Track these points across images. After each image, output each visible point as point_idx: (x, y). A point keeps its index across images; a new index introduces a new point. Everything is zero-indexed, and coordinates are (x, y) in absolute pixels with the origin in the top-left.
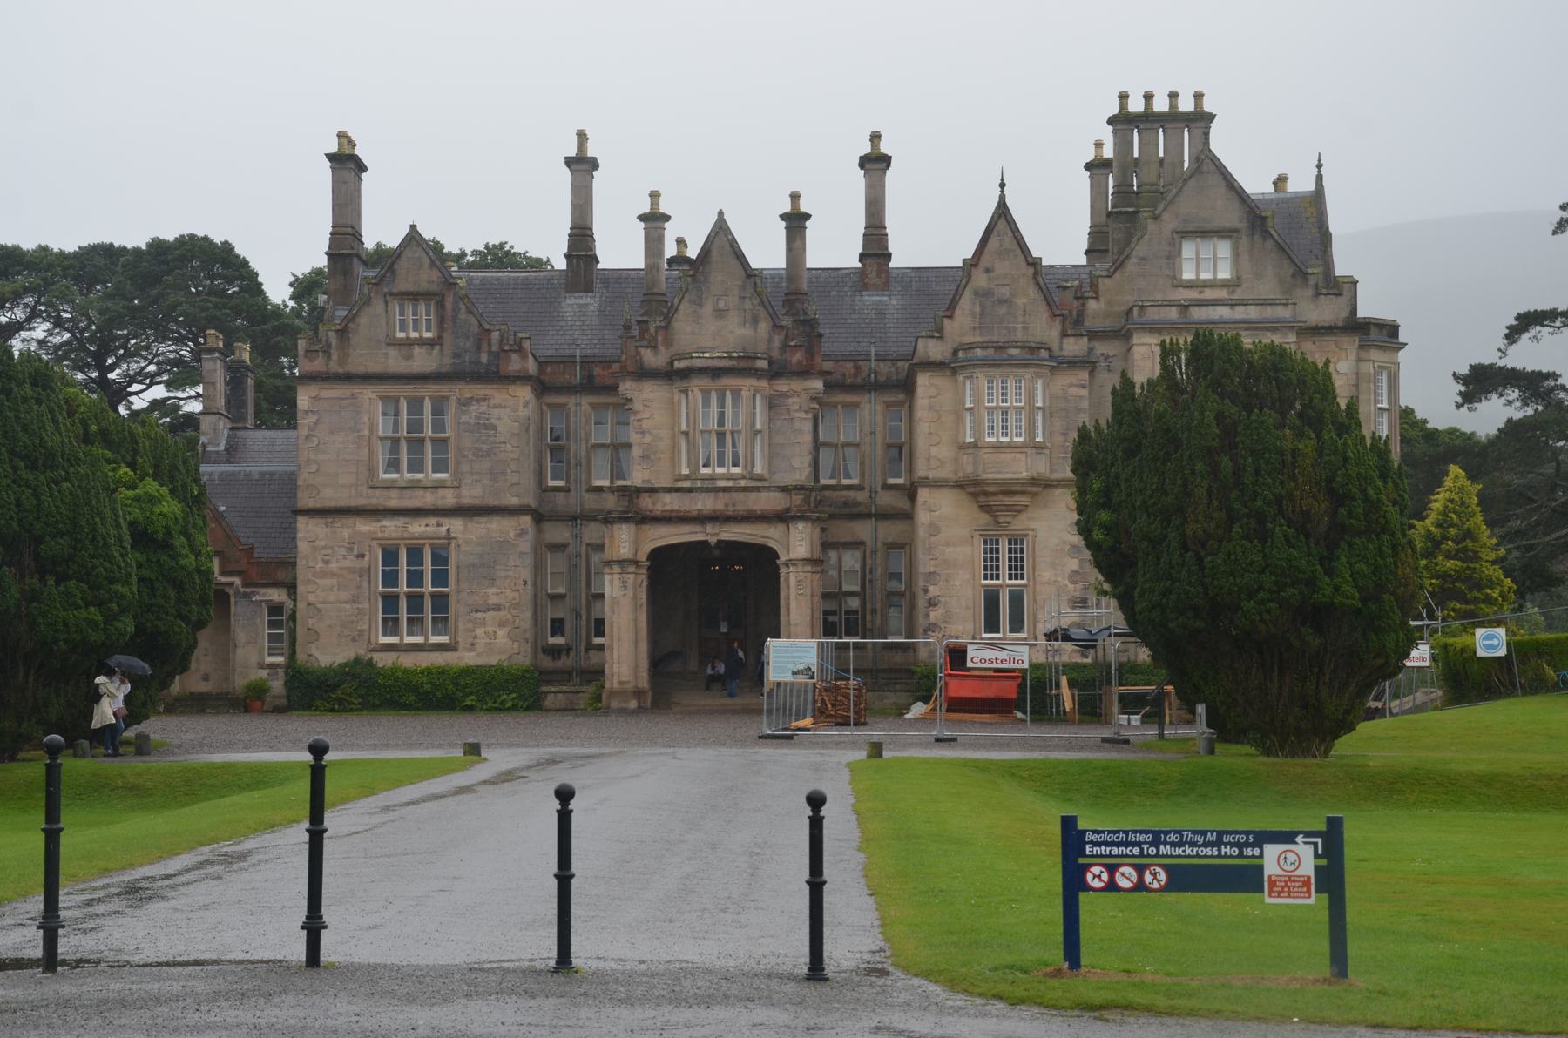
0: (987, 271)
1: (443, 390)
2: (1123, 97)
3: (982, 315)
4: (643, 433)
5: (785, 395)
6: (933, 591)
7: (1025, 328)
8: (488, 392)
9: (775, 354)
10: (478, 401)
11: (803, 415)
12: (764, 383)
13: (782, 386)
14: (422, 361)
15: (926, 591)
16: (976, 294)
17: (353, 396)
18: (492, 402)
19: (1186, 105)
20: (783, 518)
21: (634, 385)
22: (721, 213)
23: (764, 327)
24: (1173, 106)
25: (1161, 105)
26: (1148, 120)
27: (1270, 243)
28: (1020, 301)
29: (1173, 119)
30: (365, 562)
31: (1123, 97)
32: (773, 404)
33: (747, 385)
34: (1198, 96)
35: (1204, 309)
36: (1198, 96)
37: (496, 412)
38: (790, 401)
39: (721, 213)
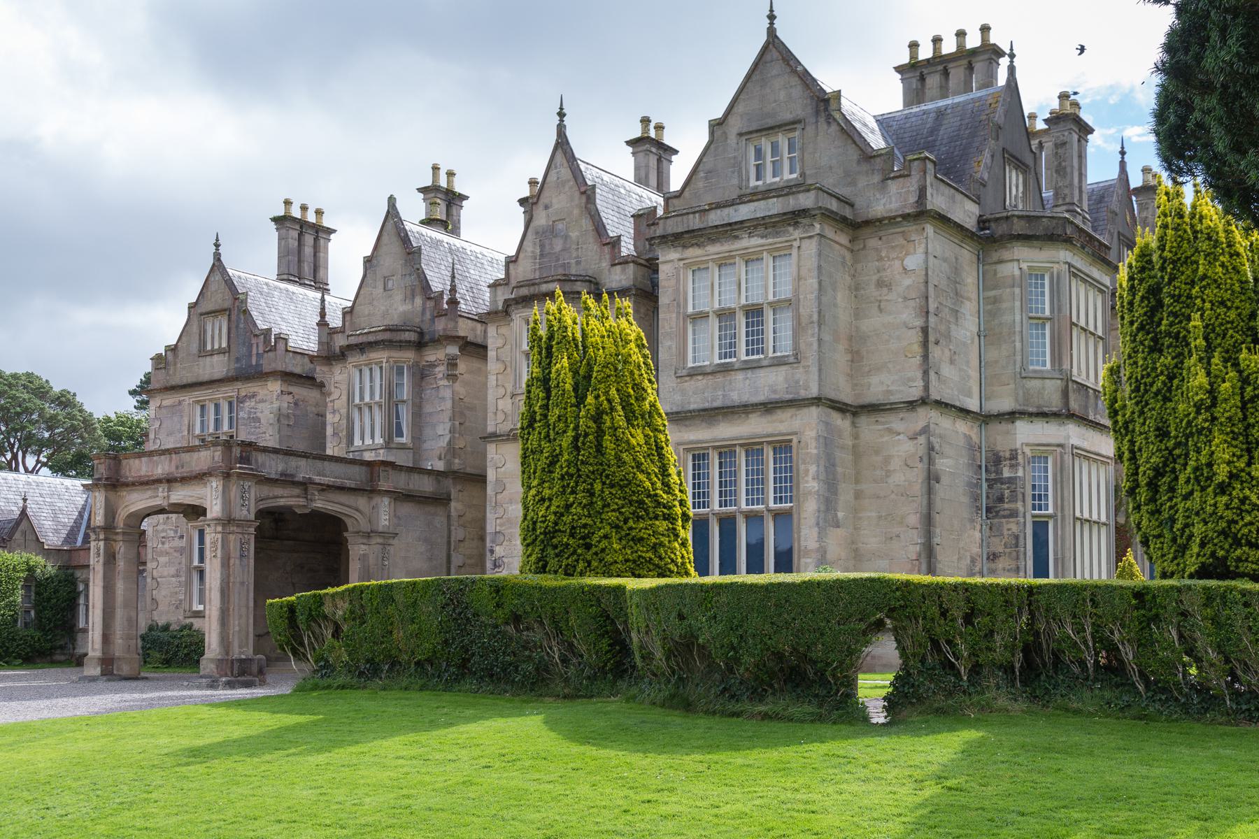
0: (546, 207)
1: (230, 391)
2: (914, 46)
3: (542, 255)
4: (334, 412)
5: (433, 365)
6: (499, 551)
7: (578, 263)
8: (255, 389)
9: (425, 327)
10: (250, 398)
11: (445, 382)
12: (409, 355)
13: (432, 355)
14: (217, 367)
15: (492, 552)
16: (537, 233)
17: (180, 403)
18: (258, 398)
19: (973, 41)
20: (200, 477)
21: (325, 369)
22: (392, 201)
23: (418, 301)
24: (961, 46)
25: (949, 47)
26: (940, 63)
27: (834, 127)
28: (574, 234)
29: (966, 57)
30: (183, 543)
31: (914, 46)
32: (421, 375)
33: (381, 355)
34: (985, 29)
35: (726, 211)
36: (985, 29)
37: (260, 406)
38: (437, 369)
39: (392, 201)
